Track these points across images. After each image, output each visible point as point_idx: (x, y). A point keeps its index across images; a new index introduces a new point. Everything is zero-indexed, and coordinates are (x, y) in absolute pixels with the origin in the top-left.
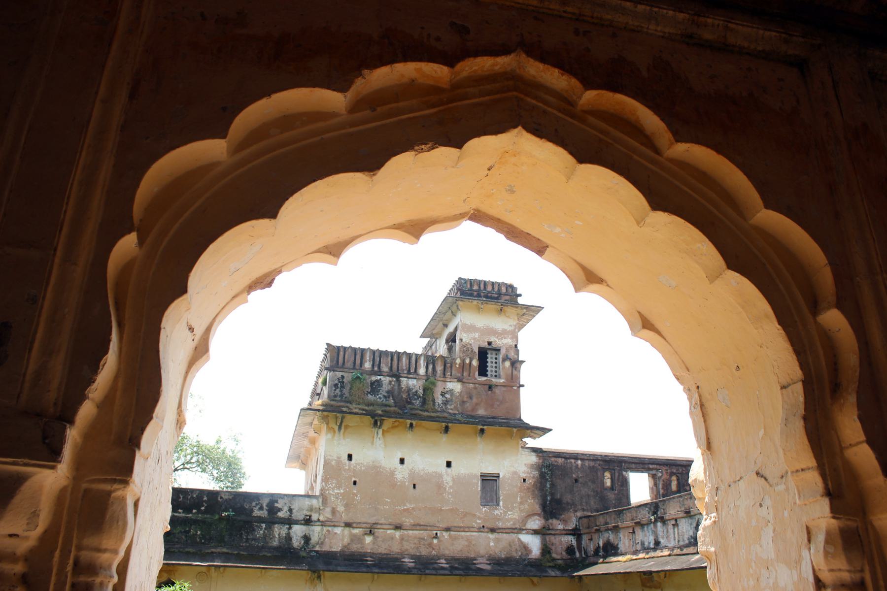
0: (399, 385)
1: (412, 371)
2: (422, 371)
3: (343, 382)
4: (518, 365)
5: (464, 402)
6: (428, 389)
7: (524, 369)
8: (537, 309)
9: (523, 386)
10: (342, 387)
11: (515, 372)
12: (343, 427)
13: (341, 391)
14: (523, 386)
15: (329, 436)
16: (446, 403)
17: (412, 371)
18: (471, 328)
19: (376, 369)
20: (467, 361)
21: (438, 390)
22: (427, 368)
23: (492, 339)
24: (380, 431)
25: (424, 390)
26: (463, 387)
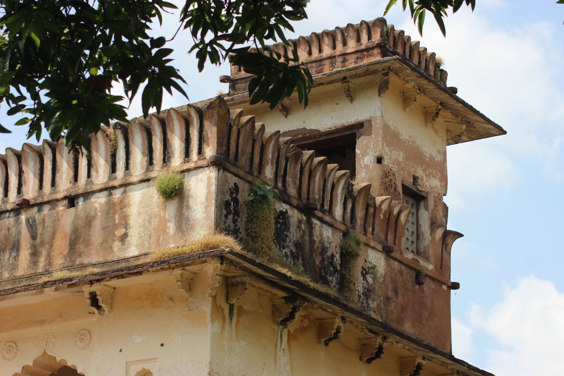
0: (311, 235)
1: (326, 207)
2: (338, 211)
3: (236, 201)
4: (449, 240)
5: (388, 299)
6: (348, 255)
7: (457, 247)
8: (504, 133)
9: (456, 286)
10: (237, 213)
11: (445, 255)
12: (235, 311)
13: (235, 221)
14: (456, 286)
15: (217, 325)
16: (368, 292)
17: (326, 207)
18: (392, 137)
19: (280, 185)
20: (395, 212)
21: (359, 264)
22: (345, 208)
23: (420, 173)
24: (285, 333)
25: (342, 255)
26: (388, 265)
